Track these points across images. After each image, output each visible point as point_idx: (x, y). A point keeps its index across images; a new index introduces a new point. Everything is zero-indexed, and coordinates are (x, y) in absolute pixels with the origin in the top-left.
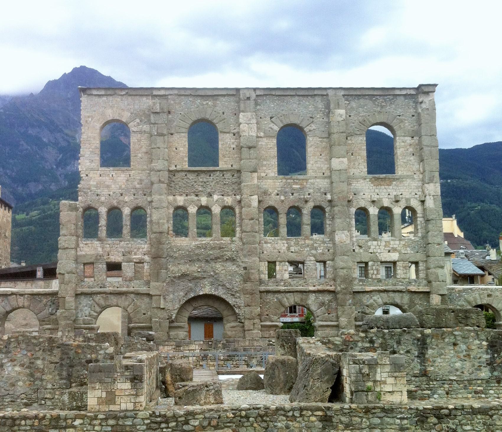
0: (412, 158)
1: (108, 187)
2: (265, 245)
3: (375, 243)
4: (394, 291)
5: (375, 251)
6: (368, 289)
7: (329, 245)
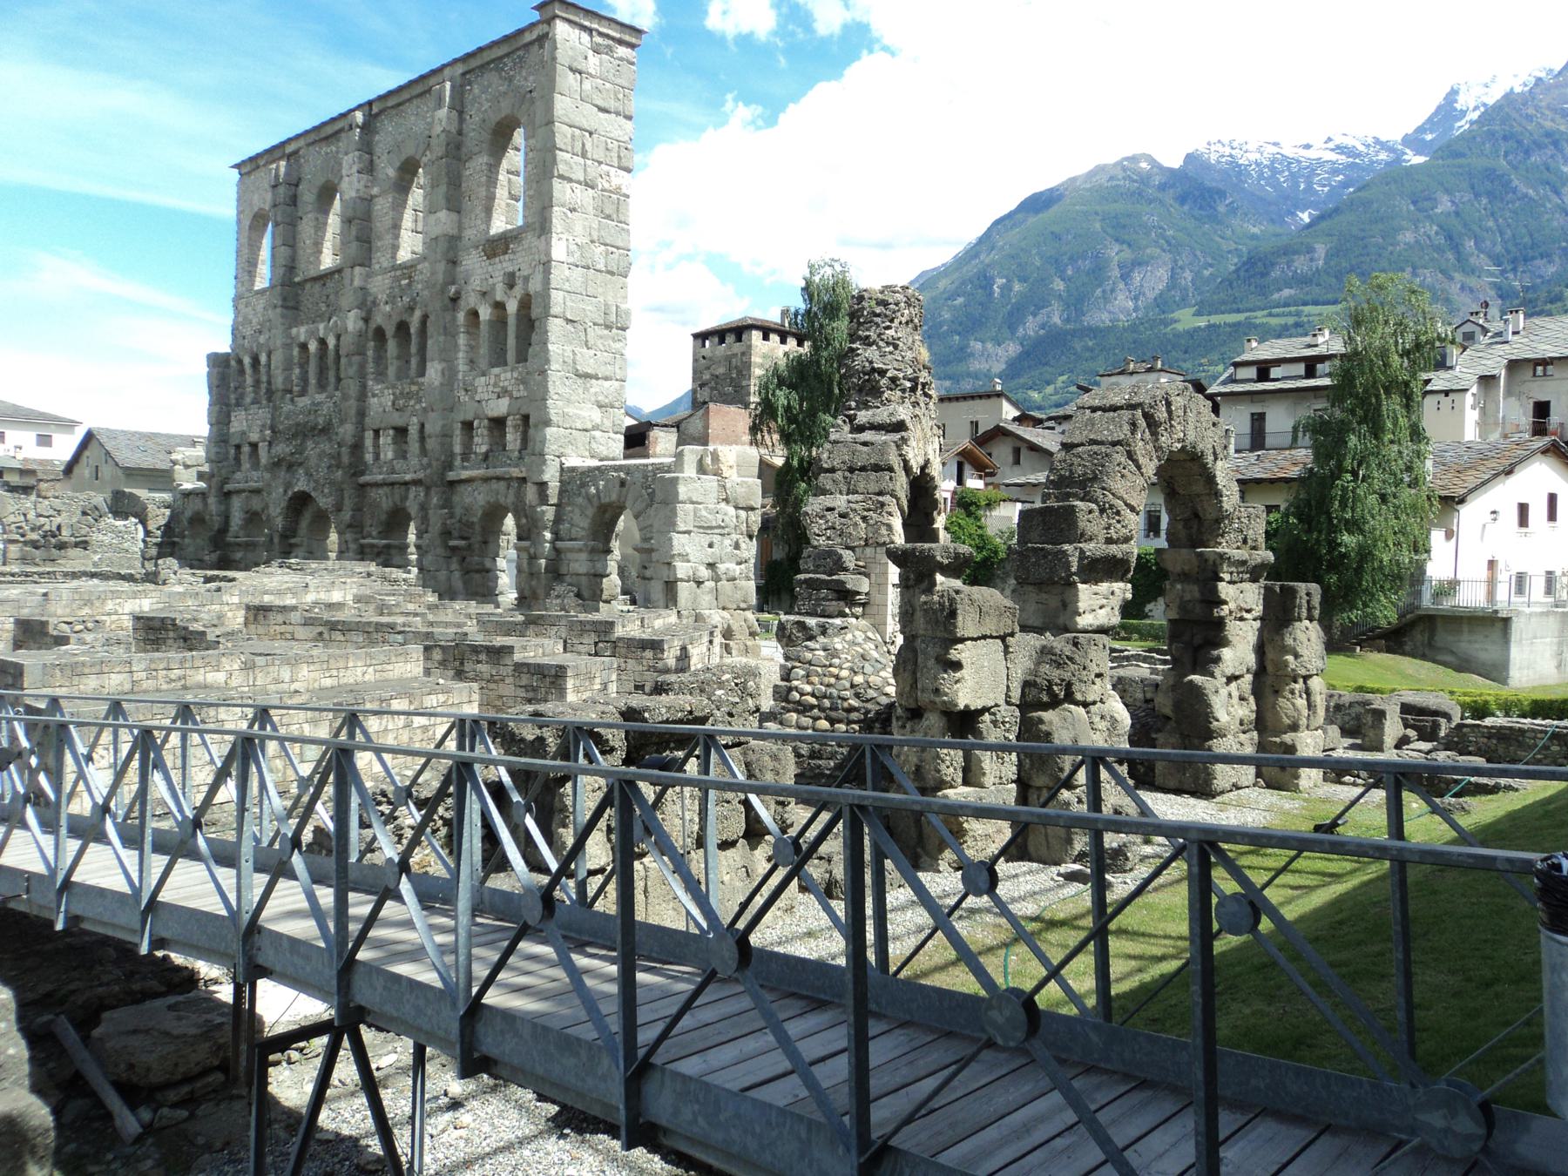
4: (498, 479)
6: (465, 474)
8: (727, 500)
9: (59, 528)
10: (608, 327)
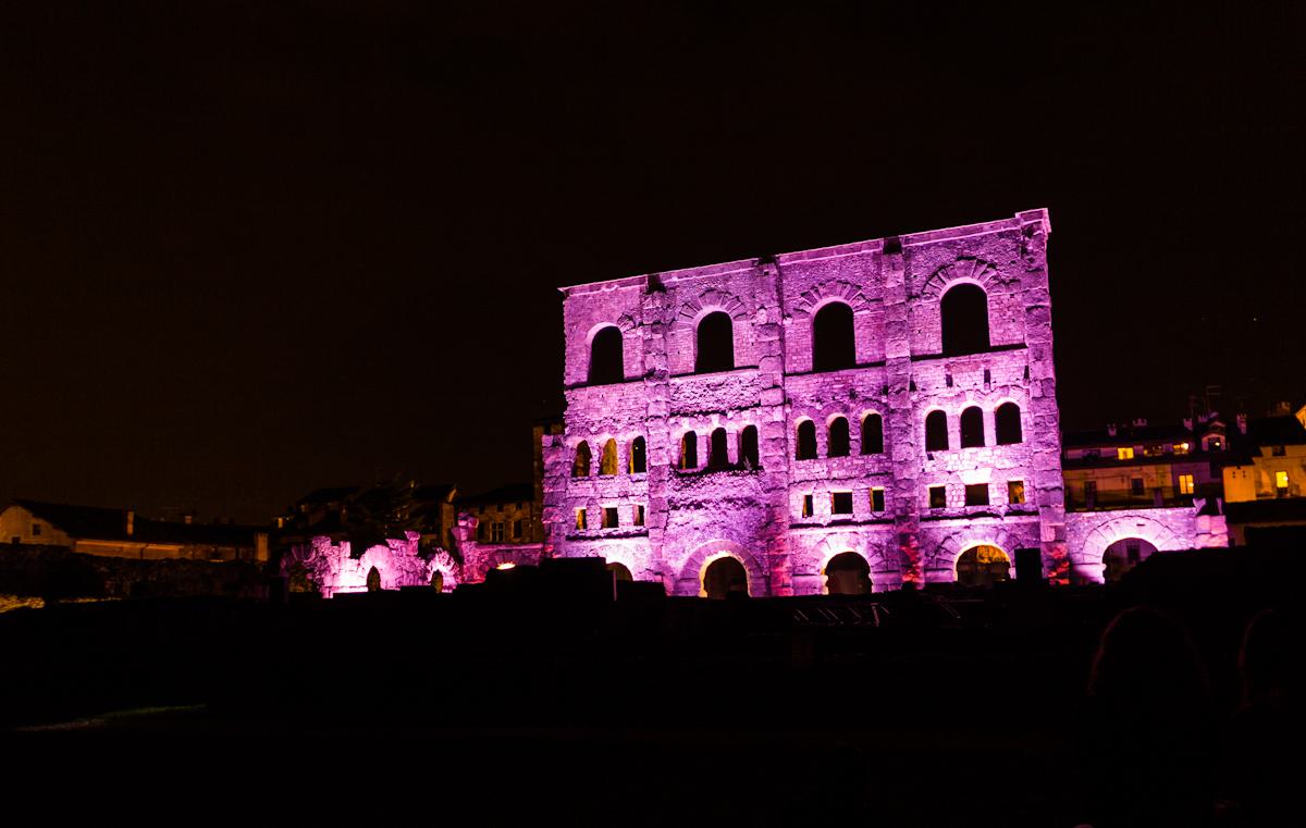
0: (1011, 326)
1: (598, 410)
2: (797, 471)
3: (955, 457)
5: (955, 468)
7: (886, 464)
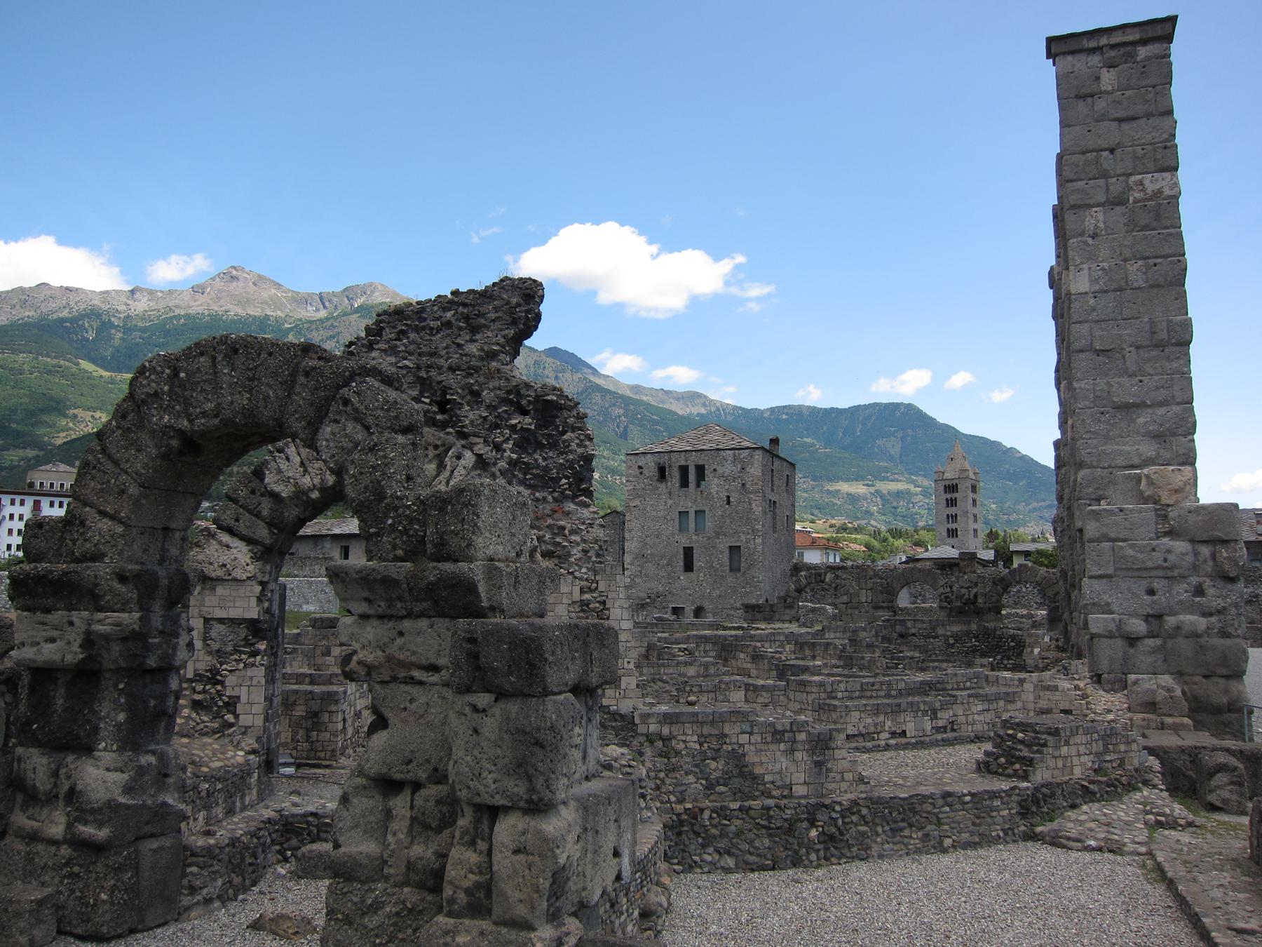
8: (1171, 533)
9: (976, 596)
10: (1160, 345)
